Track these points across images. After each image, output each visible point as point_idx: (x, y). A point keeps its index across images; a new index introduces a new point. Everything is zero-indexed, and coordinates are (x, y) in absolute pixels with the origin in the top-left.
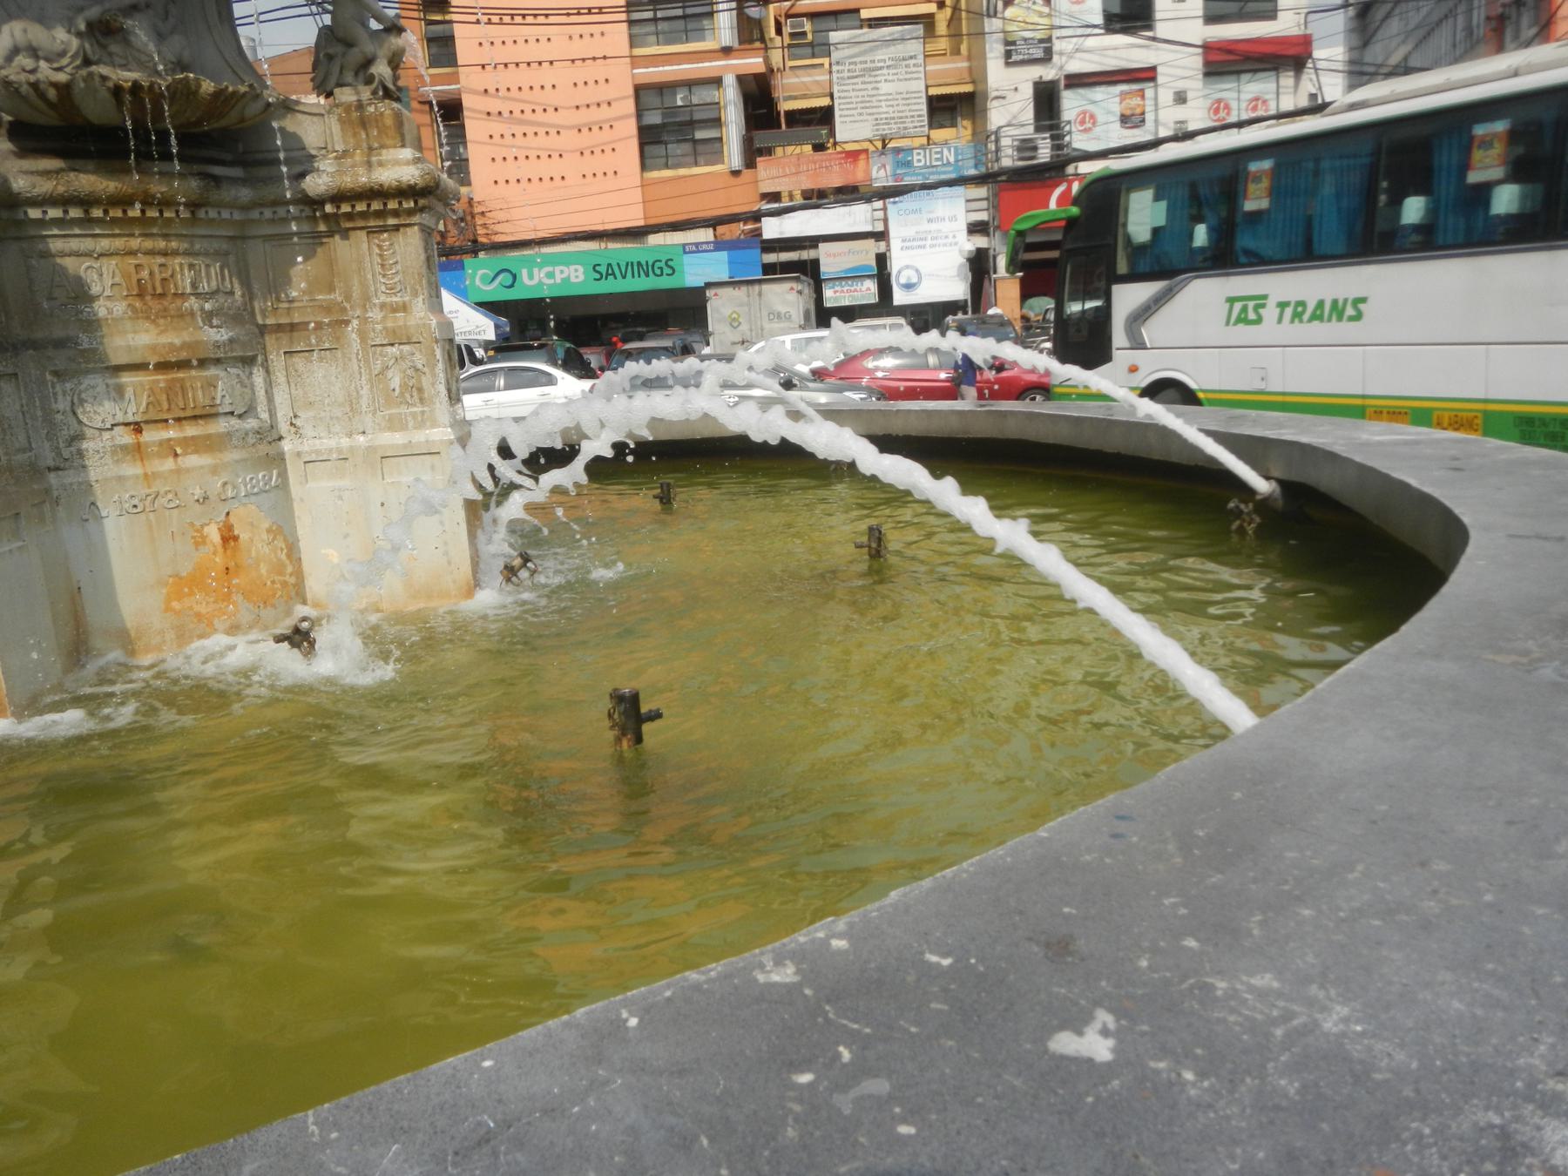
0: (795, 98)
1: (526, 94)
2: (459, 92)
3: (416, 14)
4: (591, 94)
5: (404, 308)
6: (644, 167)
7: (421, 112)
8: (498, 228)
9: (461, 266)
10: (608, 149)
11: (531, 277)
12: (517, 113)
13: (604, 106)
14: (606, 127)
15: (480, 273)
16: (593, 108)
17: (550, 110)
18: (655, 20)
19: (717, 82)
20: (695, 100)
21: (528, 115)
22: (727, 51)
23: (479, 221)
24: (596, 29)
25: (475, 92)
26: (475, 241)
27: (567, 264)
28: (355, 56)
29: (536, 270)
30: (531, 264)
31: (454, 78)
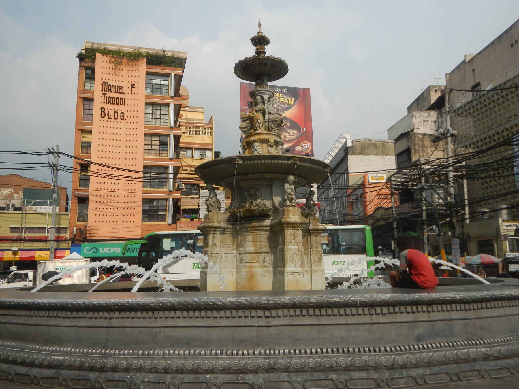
0: (185, 206)
1: (109, 197)
2: (88, 195)
3: (78, 172)
4: (129, 199)
5: (318, 248)
6: (143, 220)
7: (75, 199)
8: (94, 235)
9: (80, 246)
10: (132, 215)
11: (103, 250)
12: (105, 202)
13: (133, 203)
14: (133, 209)
15: (86, 247)
16: (129, 203)
17: (116, 202)
18: (150, 182)
19: (167, 200)
20: (159, 204)
21: (109, 203)
22: (170, 192)
23: (88, 232)
24: (133, 182)
25: (93, 195)
26: (86, 238)
27: (115, 247)
28: (312, 209)
29: (105, 248)
30: (103, 247)
31: (88, 190)
